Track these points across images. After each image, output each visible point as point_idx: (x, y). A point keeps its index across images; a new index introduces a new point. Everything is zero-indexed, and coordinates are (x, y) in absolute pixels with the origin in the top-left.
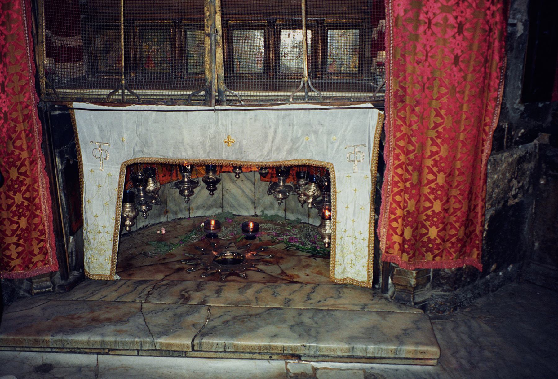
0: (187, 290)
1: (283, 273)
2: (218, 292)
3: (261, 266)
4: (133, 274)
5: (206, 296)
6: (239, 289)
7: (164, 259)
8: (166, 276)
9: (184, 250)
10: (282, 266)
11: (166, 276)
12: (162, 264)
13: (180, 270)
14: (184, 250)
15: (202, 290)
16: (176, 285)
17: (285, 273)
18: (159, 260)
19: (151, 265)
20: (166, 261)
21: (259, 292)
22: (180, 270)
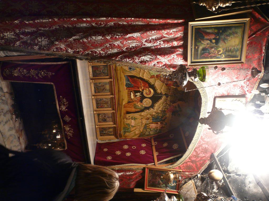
0: (3, 111)
2: (6, 123)
5: (2, 121)
8: (7, 92)
15: (5, 116)
16: (4, 104)
21: (11, 135)
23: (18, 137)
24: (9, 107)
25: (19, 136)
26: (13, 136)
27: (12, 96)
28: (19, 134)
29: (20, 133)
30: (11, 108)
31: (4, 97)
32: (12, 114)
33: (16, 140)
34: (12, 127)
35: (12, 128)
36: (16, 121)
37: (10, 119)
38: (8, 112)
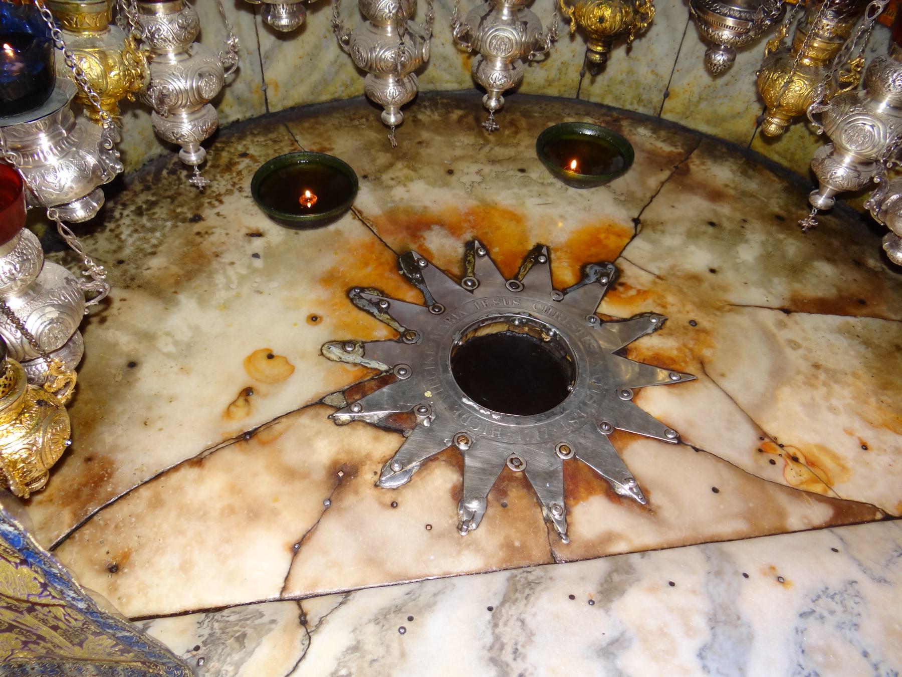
1: (766, 443)
3: (657, 402)
4: (126, 556)
6: (701, 656)
7: (247, 392)
8: (295, 550)
9: (314, 319)
10: (730, 385)
11: (295, 550)
12: (246, 437)
13: (341, 477)
14: (314, 319)
17: (774, 440)
18: (228, 413)
19: (197, 461)
20: (264, 410)
22: (341, 477)
23: (829, 525)
24: (470, 561)
25: (820, 498)
26: (816, 634)
27: (367, 476)
28: (794, 492)
29: (792, 476)
30: (488, 539)
31: (316, 639)
32: (558, 547)
33: (868, 588)
34: (700, 622)
35: (713, 621)
36: (643, 505)
37: (599, 625)
38: (510, 633)
